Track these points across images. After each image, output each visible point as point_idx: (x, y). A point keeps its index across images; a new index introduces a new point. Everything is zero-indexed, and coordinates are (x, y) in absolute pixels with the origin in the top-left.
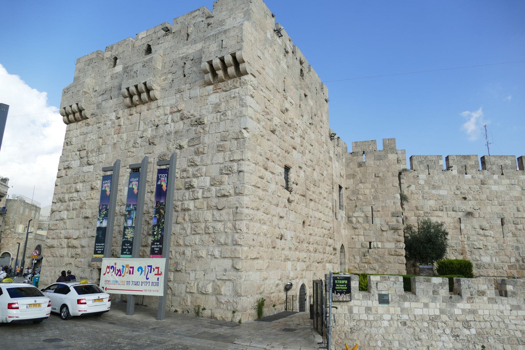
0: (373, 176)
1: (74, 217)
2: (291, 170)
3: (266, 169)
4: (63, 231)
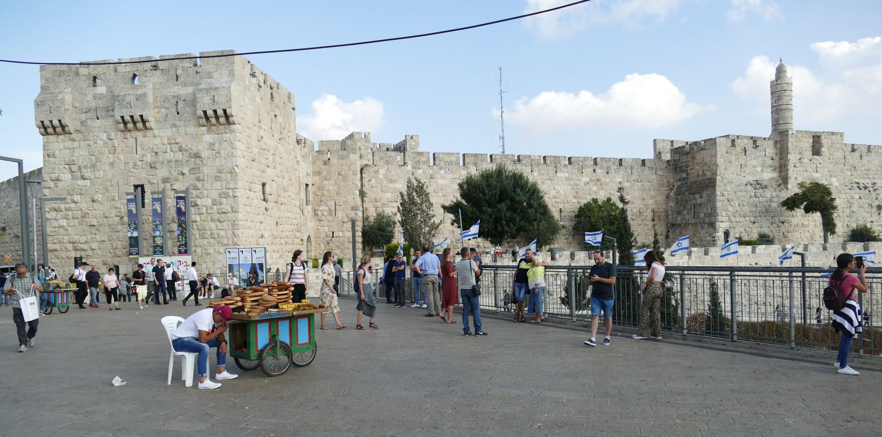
0: (337, 174)
1: (77, 225)
2: (267, 185)
3: (250, 191)
4: (65, 237)
